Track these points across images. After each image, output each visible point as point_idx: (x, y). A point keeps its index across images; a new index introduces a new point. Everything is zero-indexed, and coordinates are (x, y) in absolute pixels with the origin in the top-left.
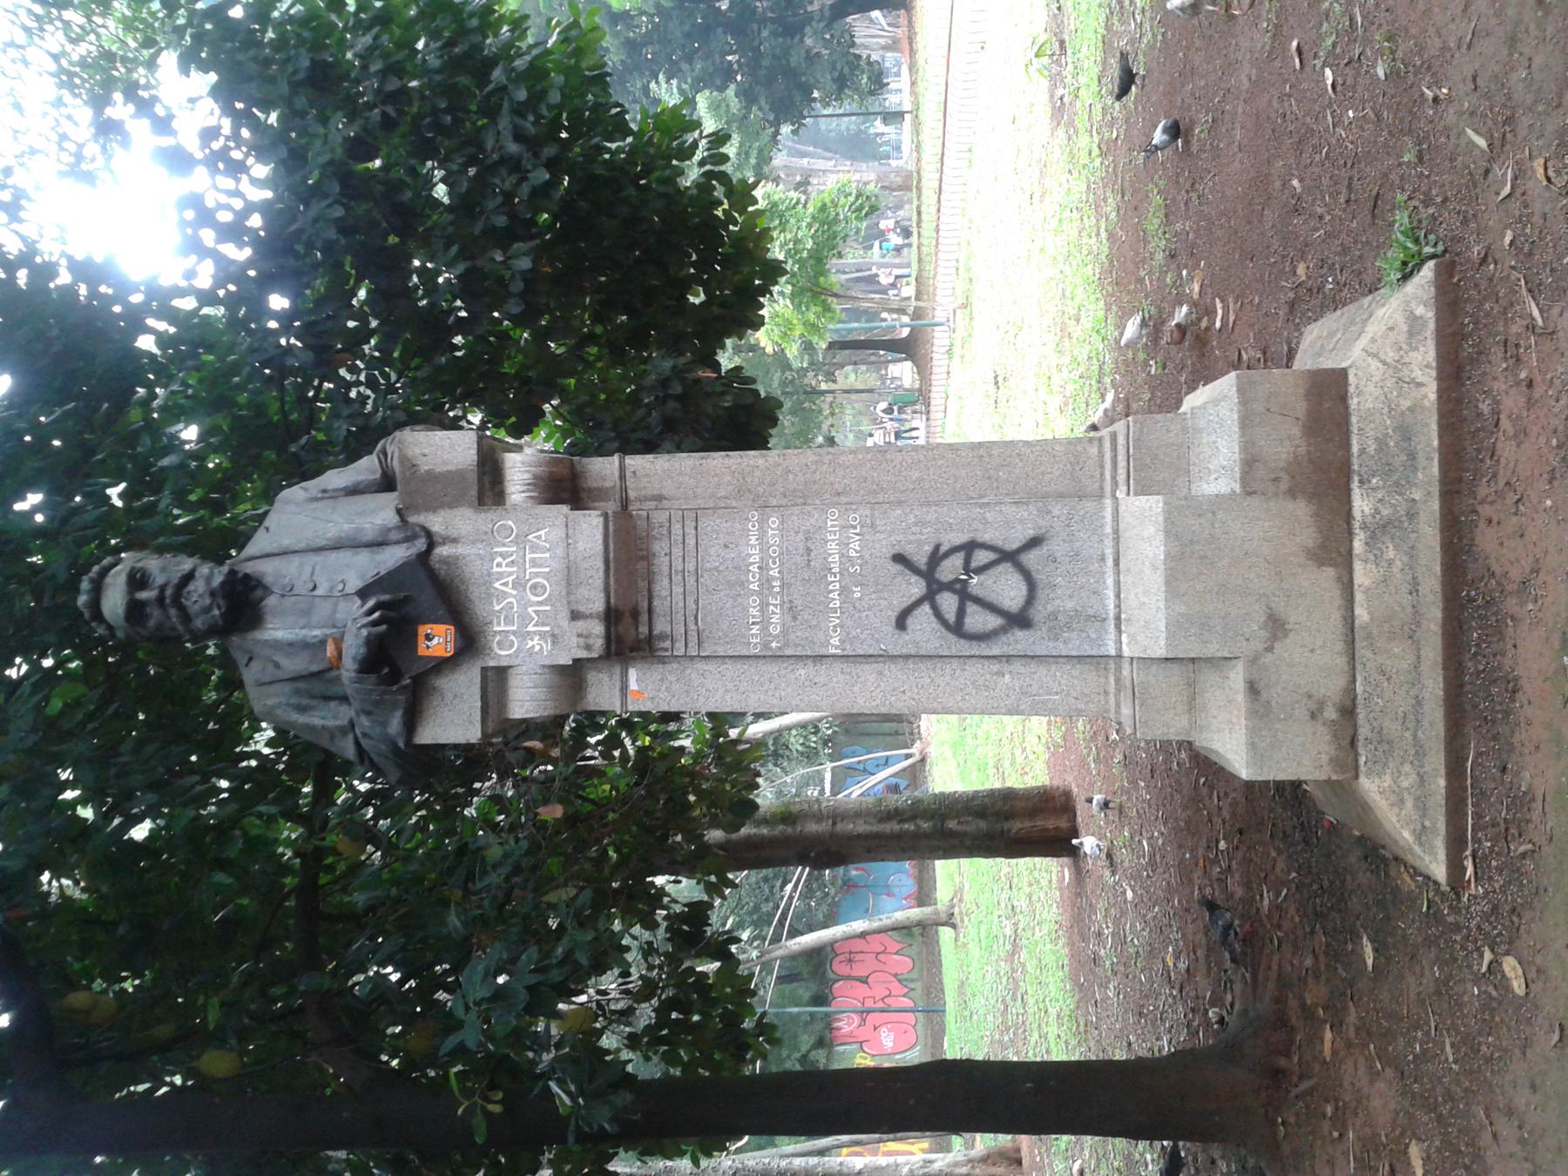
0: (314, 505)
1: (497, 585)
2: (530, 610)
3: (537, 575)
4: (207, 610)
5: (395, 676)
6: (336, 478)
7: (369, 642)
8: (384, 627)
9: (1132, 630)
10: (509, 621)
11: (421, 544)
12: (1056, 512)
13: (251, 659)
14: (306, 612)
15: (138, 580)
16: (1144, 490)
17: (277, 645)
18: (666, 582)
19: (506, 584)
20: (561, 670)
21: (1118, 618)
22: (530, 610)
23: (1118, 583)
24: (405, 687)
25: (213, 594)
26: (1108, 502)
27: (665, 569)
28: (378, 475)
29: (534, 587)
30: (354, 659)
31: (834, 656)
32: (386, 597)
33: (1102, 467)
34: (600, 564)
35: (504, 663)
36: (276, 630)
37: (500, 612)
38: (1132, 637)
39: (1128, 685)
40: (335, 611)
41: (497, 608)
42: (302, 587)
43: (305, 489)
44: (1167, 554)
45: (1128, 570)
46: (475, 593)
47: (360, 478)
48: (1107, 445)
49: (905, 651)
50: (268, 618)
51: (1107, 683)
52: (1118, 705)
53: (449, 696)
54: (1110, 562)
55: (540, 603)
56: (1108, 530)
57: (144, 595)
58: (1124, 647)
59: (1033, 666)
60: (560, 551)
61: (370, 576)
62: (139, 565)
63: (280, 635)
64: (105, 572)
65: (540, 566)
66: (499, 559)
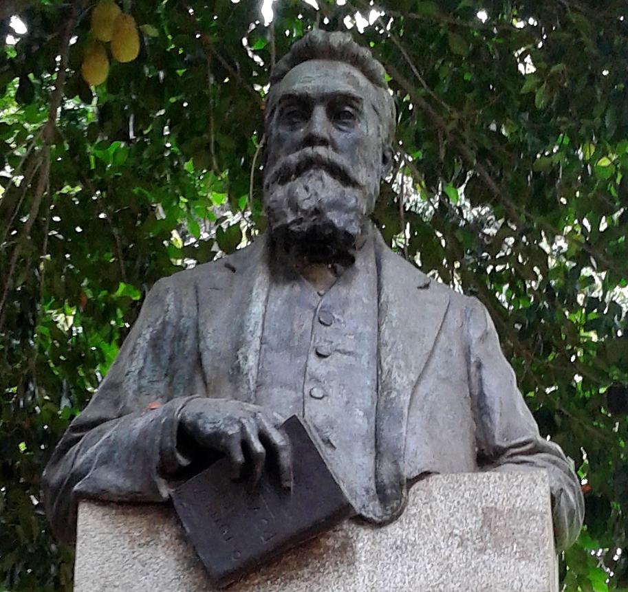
4: (295, 207)
5: (175, 475)
6: (501, 381)
7: (218, 435)
8: (240, 458)
11: (373, 510)
13: (234, 270)
14: (289, 345)
15: (342, 108)
17: (243, 305)
24: (157, 492)
25: (317, 211)
28: (500, 442)
32: (286, 459)
36: (264, 302)
40: (284, 385)
42: (324, 338)
43: (484, 337)
47: (497, 418)
50: (285, 291)
53: (145, 554)
57: (320, 114)
62: (366, 109)
63: (257, 308)
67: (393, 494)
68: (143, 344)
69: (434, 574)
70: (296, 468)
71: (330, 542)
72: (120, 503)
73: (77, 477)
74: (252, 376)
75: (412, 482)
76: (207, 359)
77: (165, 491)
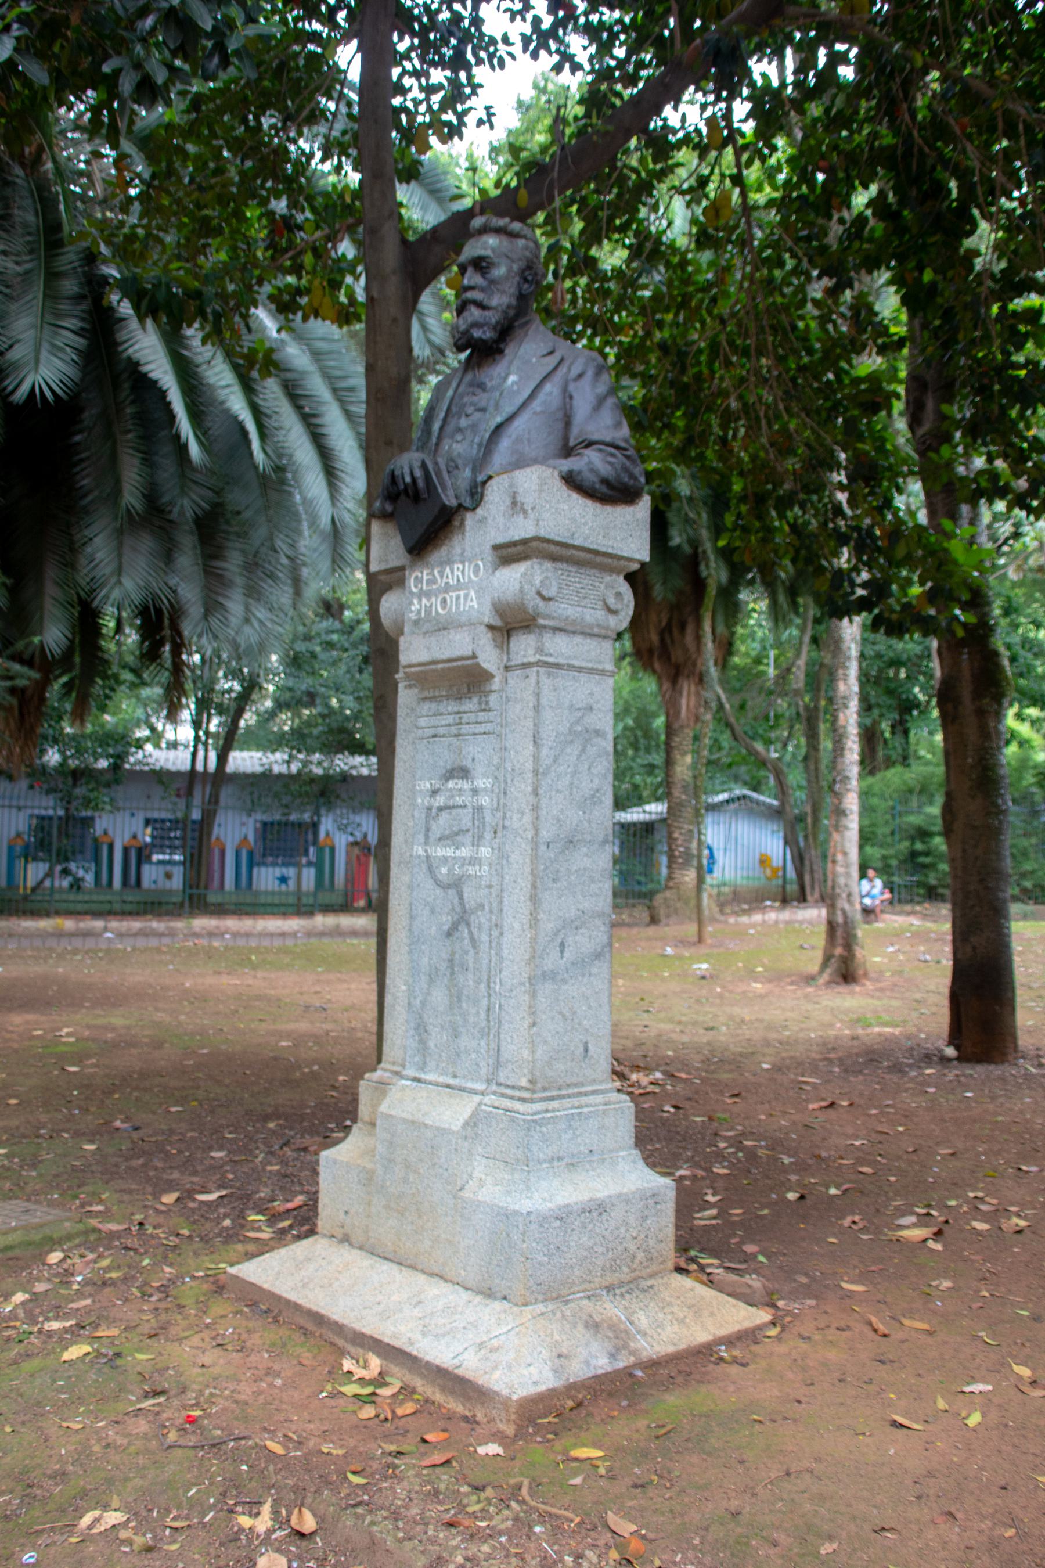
10: (428, 582)
21: (419, 1080)
23: (437, 1084)
26: (480, 1086)
27: (463, 708)
32: (421, 484)
33: (513, 1087)
34: (446, 655)
38: (404, 1088)
44: (426, 1126)
46: (442, 553)
56: (469, 1085)
60: (463, 619)
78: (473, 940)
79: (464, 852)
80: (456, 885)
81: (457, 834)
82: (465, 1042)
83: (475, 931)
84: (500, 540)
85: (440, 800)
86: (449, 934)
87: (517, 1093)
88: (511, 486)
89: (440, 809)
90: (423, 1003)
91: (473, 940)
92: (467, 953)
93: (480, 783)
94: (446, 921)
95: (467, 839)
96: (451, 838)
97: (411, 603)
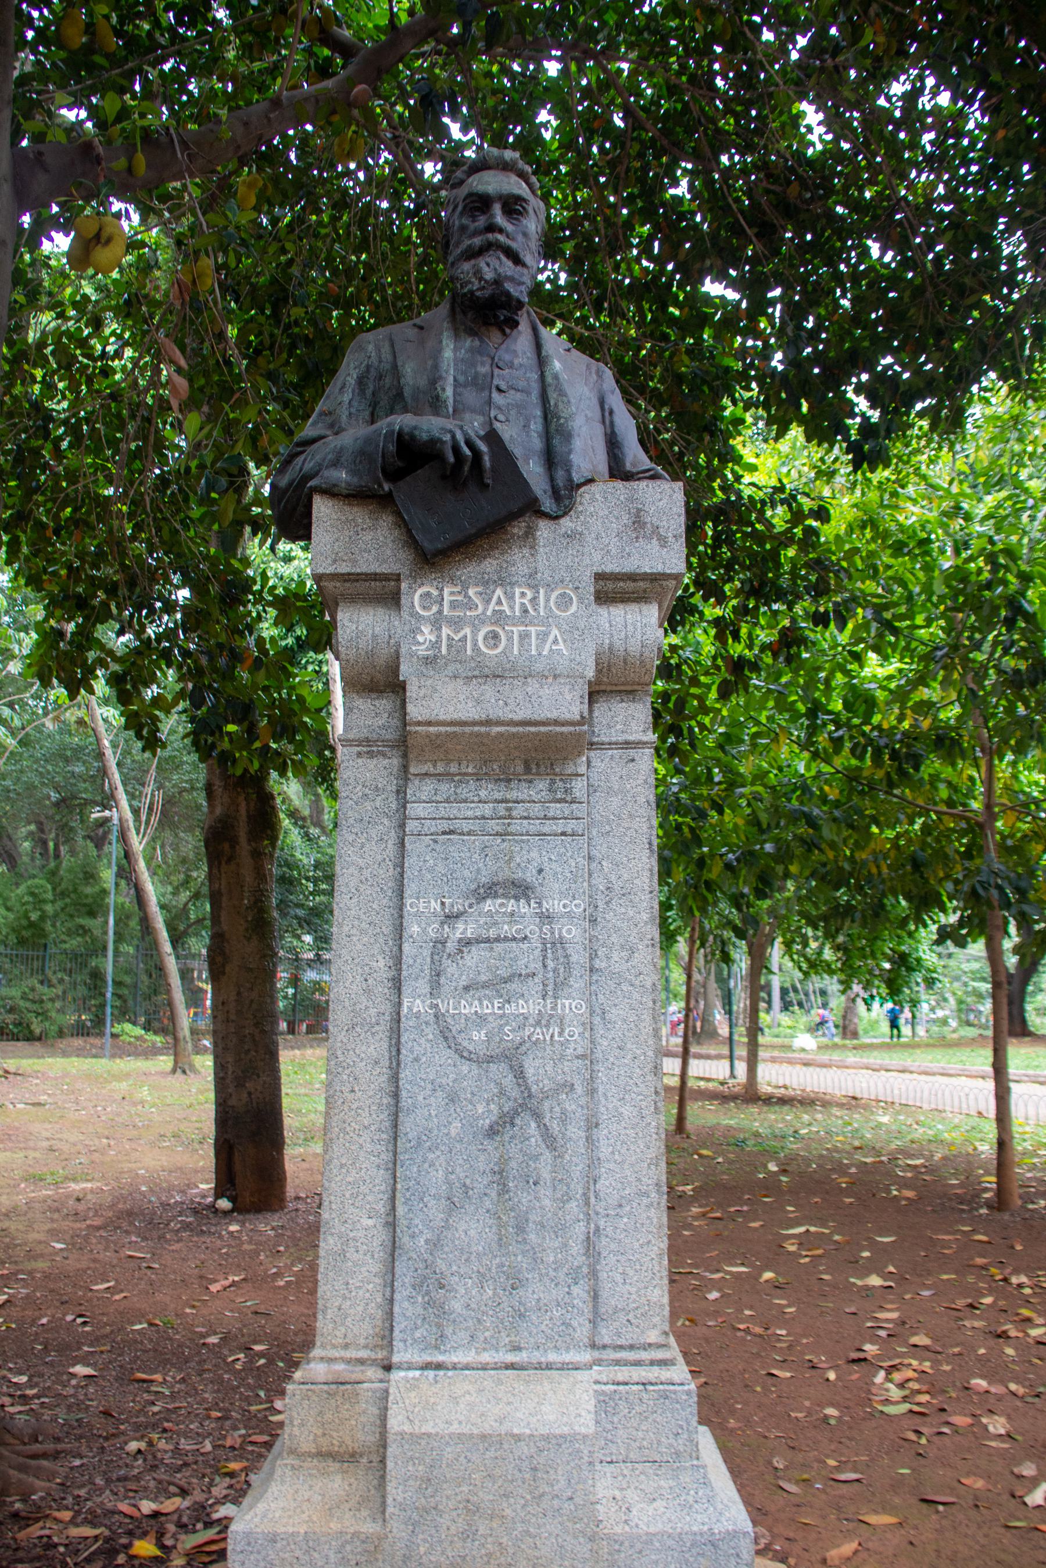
0: (595, 402)
1: (499, 592)
2: (467, 631)
3: (510, 639)
4: (478, 273)
7: (434, 442)
8: (451, 459)
9: (424, 1386)
10: (453, 605)
12: (576, 1290)
16: (605, 1404)
17: (438, 351)
18: (498, 796)
19: (499, 602)
20: (394, 667)
21: (439, 1366)
22: (467, 631)
23: (484, 1367)
25: (497, 282)
27: (513, 795)
29: (495, 636)
30: (415, 428)
31: (400, 1004)
33: (632, 1347)
34: (519, 716)
35: (403, 601)
36: (450, 352)
37: (466, 596)
39: (354, 1377)
41: (471, 592)
44: (518, 1438)
45: (500, 1382)
46: (490, 565)
48: (659, 1355)
49: (404, 1094)
51: (358, 1347)
52: (331, 1360)
54: (510, 1358)
55: (475, 644)
56: (552, 1357)
57: (497, 209)
58: (402, 1374)
59: (380, 1255)
60: (538, 667)
61: (517, 451)
63: (448, 354)
64: (522, 175)
65: (521, 645)
66: (529, 595)
67: (565, 494)
68: (352, 381)
69: (597, 556)
70: (493, 469)
71: (515, 530)
72: (347, 496)
73: (307, 478)
74: (450, 402)
75: (580, 486)
76: (407, 392)
77: (386, 487)
78: (549, 1140)
79: (529, 1006)
80: (512, 1058)
81: (506, 981)
82: (534, 1292)
83: (555, 1127)
84: (611, 567)
85: (464, 929)
86: (492, 1132)
87: (644, 1355)
88: (631, 500)
89: (466, 943)
90: (435, 1244)
91: (549, 1140)
92: (536, 1158)
93: (555, 905)
94: (486, 1112)
95: (534, 986)
96: (499, 985)
97: (415, 631)
